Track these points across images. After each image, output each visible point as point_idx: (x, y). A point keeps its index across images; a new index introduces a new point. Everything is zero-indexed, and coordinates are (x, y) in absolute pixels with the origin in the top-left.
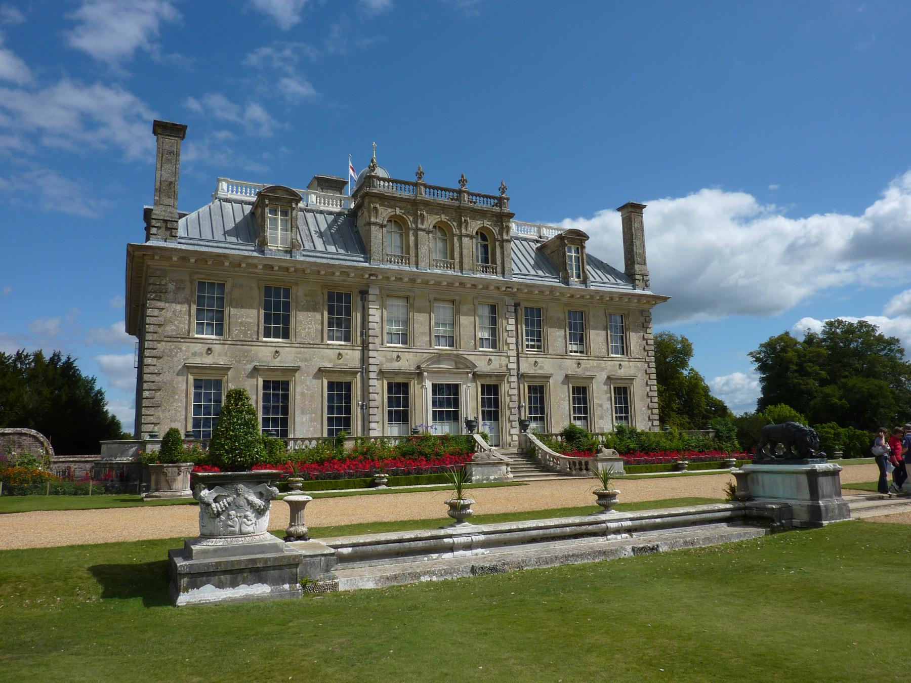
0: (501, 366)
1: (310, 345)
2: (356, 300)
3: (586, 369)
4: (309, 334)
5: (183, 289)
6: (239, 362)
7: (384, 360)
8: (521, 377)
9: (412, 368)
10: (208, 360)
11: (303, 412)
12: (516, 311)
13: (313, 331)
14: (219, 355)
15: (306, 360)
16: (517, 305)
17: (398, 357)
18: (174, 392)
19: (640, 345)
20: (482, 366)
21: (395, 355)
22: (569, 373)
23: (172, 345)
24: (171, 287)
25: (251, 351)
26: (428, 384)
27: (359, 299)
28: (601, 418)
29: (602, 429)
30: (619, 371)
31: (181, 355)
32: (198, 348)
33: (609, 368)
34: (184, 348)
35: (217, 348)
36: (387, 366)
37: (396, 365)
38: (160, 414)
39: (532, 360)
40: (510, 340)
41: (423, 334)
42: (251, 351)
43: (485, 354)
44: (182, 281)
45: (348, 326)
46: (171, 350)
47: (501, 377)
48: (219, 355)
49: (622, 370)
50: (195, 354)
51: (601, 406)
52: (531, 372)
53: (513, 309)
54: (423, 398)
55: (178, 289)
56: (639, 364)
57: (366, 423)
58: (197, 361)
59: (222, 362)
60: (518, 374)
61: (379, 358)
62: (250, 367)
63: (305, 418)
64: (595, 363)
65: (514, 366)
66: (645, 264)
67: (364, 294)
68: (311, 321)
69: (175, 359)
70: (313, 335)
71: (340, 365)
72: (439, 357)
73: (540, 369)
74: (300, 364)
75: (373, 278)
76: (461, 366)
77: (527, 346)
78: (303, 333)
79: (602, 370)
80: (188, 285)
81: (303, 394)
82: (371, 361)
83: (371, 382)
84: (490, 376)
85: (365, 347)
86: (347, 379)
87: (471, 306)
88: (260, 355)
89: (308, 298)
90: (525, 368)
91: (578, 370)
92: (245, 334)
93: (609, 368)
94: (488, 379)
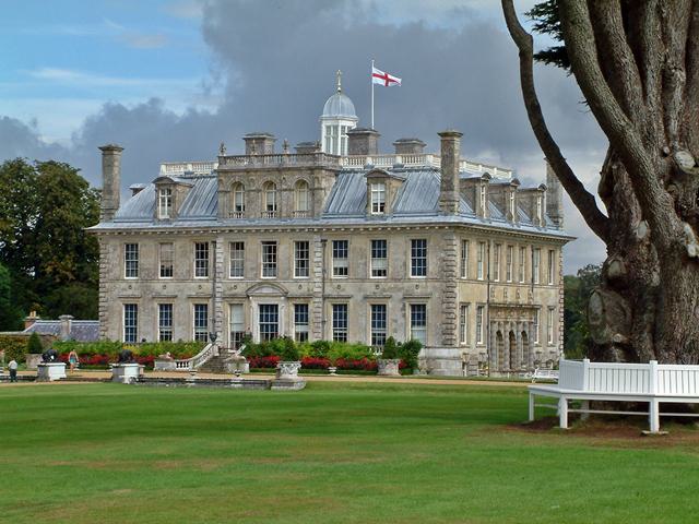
1: (183, 281)
2: (211, 247)
3: (384, 290)
8: (325, 298)
10: (130, 292)
11: (179, 325)
16: (324, 241)
20: (293, 290)
23: (112, 285)
24: (111, 250)
28: (395, 331)
32: (124, 285)
35: (134, 285)
39: (336, 285)
47: (310, 297)
49: (419, 291)
50: (124, 289)
51: (396, 321)
52: (335, 294)
53: (320, 245)
54: (286, 313)
58: (125, 293)
59: (137, 293)
61: (220, 287)
63: (180, 328)
64: (392, 285)
65: (320, 290)
72: (261, 284)
78: (179, 273)
79: (399, 290)
81: (179, 313)
82: (217, 290)
83: (217, 305)
85: (215, 281)
90: (329, 290)
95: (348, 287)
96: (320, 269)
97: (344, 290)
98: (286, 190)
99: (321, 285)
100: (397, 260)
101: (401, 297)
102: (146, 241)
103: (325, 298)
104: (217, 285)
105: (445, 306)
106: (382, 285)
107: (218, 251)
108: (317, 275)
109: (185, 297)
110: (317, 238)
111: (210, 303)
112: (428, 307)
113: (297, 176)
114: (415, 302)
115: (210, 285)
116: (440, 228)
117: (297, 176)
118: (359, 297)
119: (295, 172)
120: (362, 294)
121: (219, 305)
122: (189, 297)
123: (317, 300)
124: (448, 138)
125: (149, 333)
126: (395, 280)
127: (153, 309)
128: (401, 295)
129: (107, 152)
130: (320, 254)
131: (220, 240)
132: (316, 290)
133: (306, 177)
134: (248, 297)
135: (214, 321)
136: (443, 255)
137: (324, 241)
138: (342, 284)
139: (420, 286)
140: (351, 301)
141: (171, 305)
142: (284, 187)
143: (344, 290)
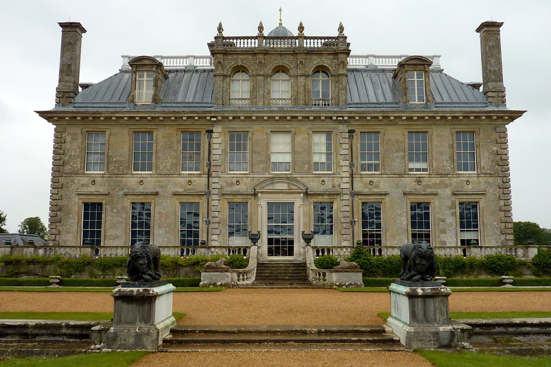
0: (334, 186)
2: (204, 139)
3: (428, 186)
4: (165, 167)
5: (77, 139)
6: (114, 190)
7: (224, 184)
8: (354, 194)
9: (250, 191)
10: (92, 189)
11: (160, 227)
12: (351, 137)
13: (168, 164)
14: (100, 185)
15: (162, 187)
16: (351, 132)
17: (237, 182)
18: (69, 213)
19: (493, 161)
20: (314, 186)
21: (234, 180)
22: (408, 190)
24: (68, 139)
25: (122, 181)
26: (263, 202)
27: (206, 136)
28: (443, 232)
29: (444, 242)
30: (466, 187)
31: (74, 187)
32: (84, 180)
33: (454, 184)
34: (76, 182)
35: (98, 180)
36: (228, 190)
37: (235, 188)
38: (60, 228)
39: (367, 180)
40: (342, 163)
41: (260, 162)
42: (122, 181)
43: (319, 176)
44: (76, 134)
45: (198, 159)
46: (67, 183)
48: (100, 185)
49: (470, 187)
50: (83, 185)
51: (444, 221)
52: (366, 191)
53: (347, 135)
55: (73, 139)
56: (491, 180)
57: (210, 235)
58: (85, 190)
60: (351, 193)
62: (121, 193)
65: (347, 186)
66: (501, 80)
67: (210, 132)
68: (167, 157)
69: (70, 189)
70: (169, 167)
71: (190, 189)
72: (273, 180)
73: (375, 187)
74: (158, 190)
75: (213, 119)
76: (294, 187)
77: (363, 168)
78: (161, 166)
79: (446, 186)
80: (80, 136)
81: (160, 213)
84: (322, 195)
85: (209, 175)
86: (195, 200)
87: (307, 136)
88: (128, 184)
89: (166, 140)
90: (358, 187)
91: (418, 187)
92: (118, 170)
93: (454, 184)
94: (320, 197)
95: (384, 184)
96: (347, 163)
97: (377, 187)
98: (302, 75)
99: (348, 180)
100: (442, 153)
101: (450, 193)
102: (116, 130)
103: (354, 194)
104: (213, 180)
105: (502, 203)
106: (425, 181)
107: (214, 141)
108: (345, 169)
109: (170, 193)
110: (344, 128)
111: (203, 201)
112: (481, 204)
113: (316, 61)
114: (465, 199)
115: (204, 180)
116: (498, 118)
117: (316, 61)
118: (396, 194)
119: (314, 57)
120: (401, 190)
121: (216, 203)
122: (175, 194)
123: (345, 197)
124: (493, 29)
125: (116, 237)
126: (441, 175)
127: (123, 208)
128: (448, 191)
129: (68, 29)
130: (347, 146)
131: (217, 129)
132: (343, 186)
133: (326, 61)
134: (255, 195)
135: (208, 223)
136: (495, 148)
137: (351, 132)
138: (375, 180)
139: (471, 181)
140: (387, 198)
141: (150, 203)
142: (300, 72)
143: (377, 187)
